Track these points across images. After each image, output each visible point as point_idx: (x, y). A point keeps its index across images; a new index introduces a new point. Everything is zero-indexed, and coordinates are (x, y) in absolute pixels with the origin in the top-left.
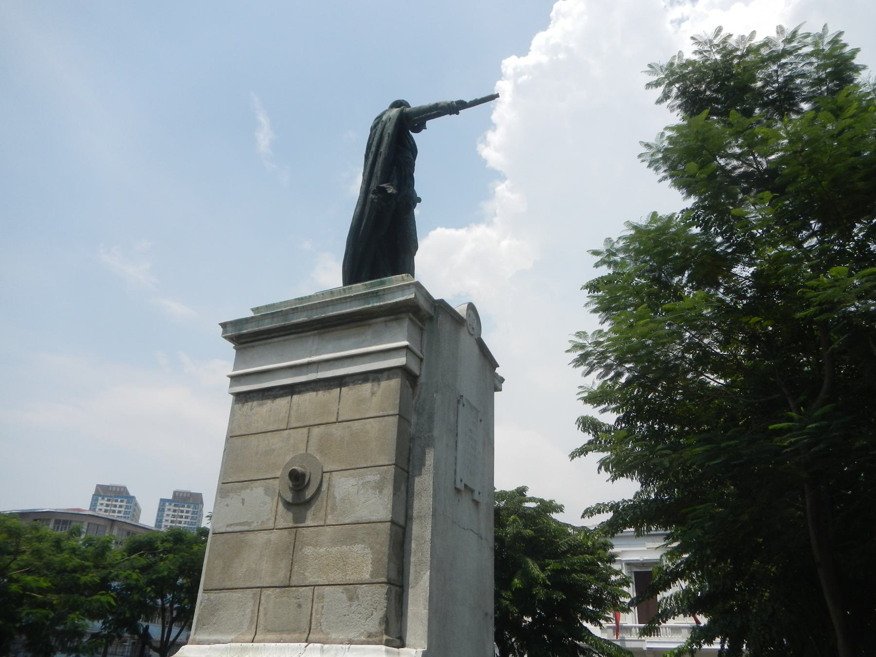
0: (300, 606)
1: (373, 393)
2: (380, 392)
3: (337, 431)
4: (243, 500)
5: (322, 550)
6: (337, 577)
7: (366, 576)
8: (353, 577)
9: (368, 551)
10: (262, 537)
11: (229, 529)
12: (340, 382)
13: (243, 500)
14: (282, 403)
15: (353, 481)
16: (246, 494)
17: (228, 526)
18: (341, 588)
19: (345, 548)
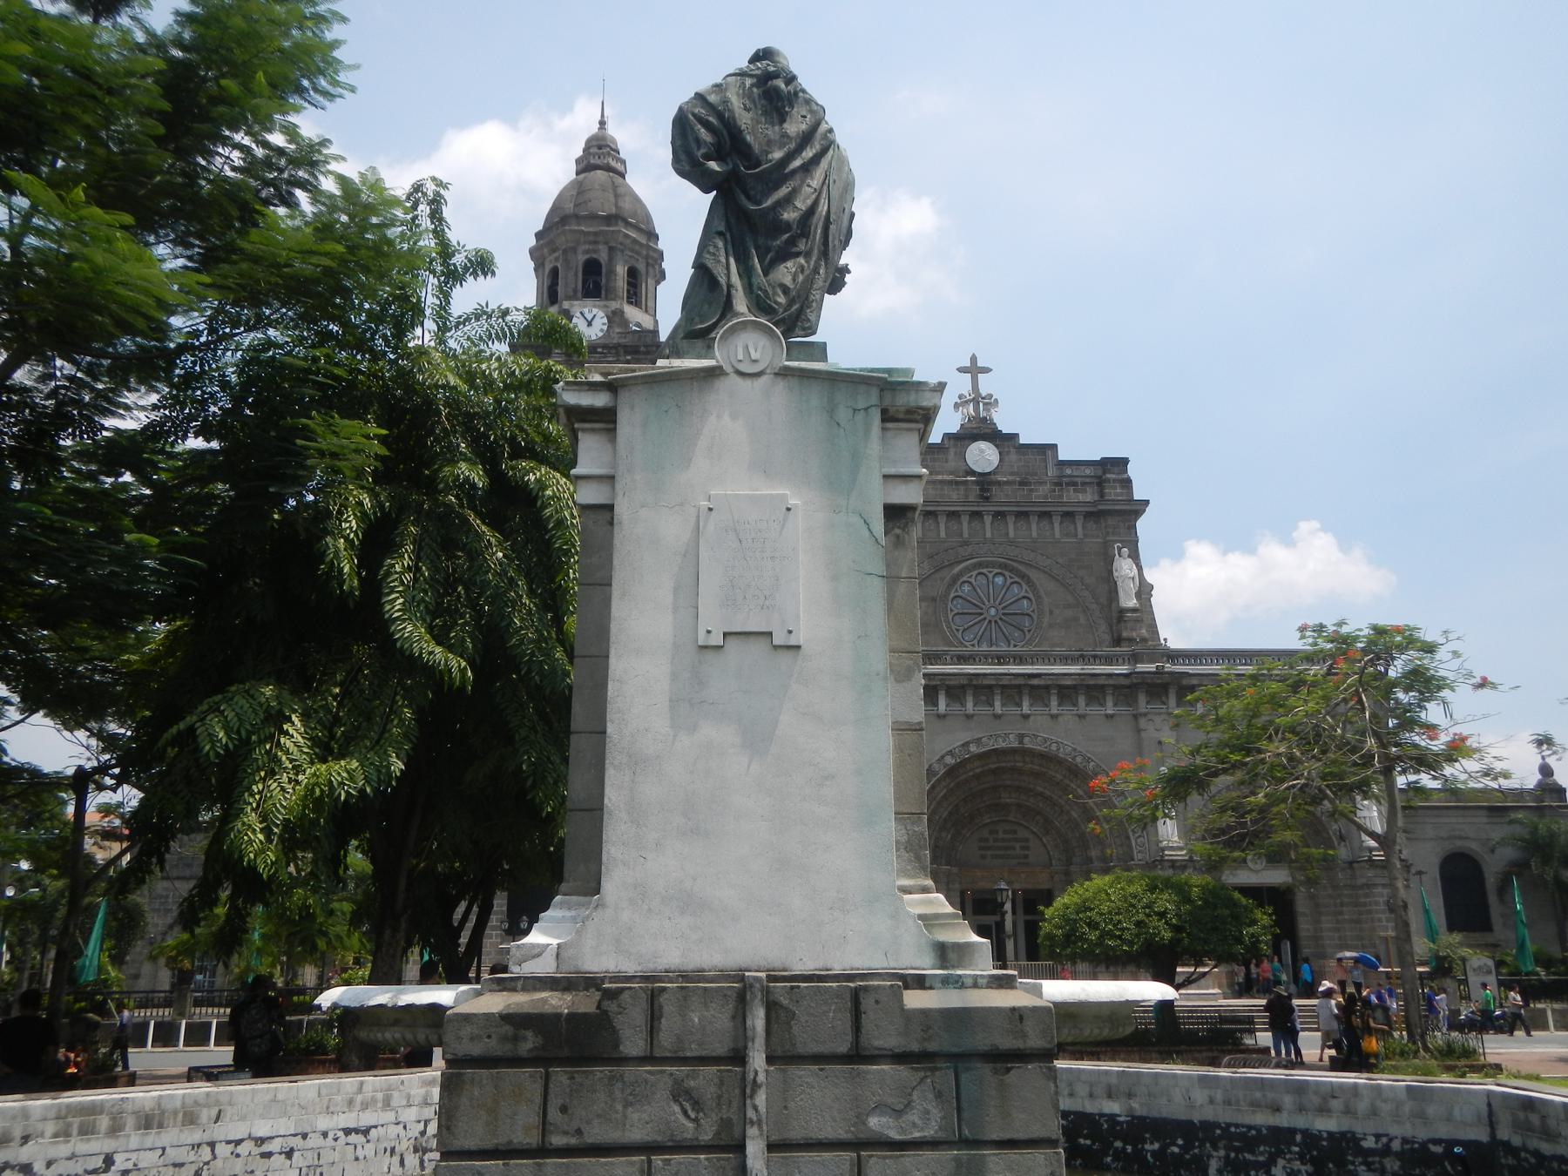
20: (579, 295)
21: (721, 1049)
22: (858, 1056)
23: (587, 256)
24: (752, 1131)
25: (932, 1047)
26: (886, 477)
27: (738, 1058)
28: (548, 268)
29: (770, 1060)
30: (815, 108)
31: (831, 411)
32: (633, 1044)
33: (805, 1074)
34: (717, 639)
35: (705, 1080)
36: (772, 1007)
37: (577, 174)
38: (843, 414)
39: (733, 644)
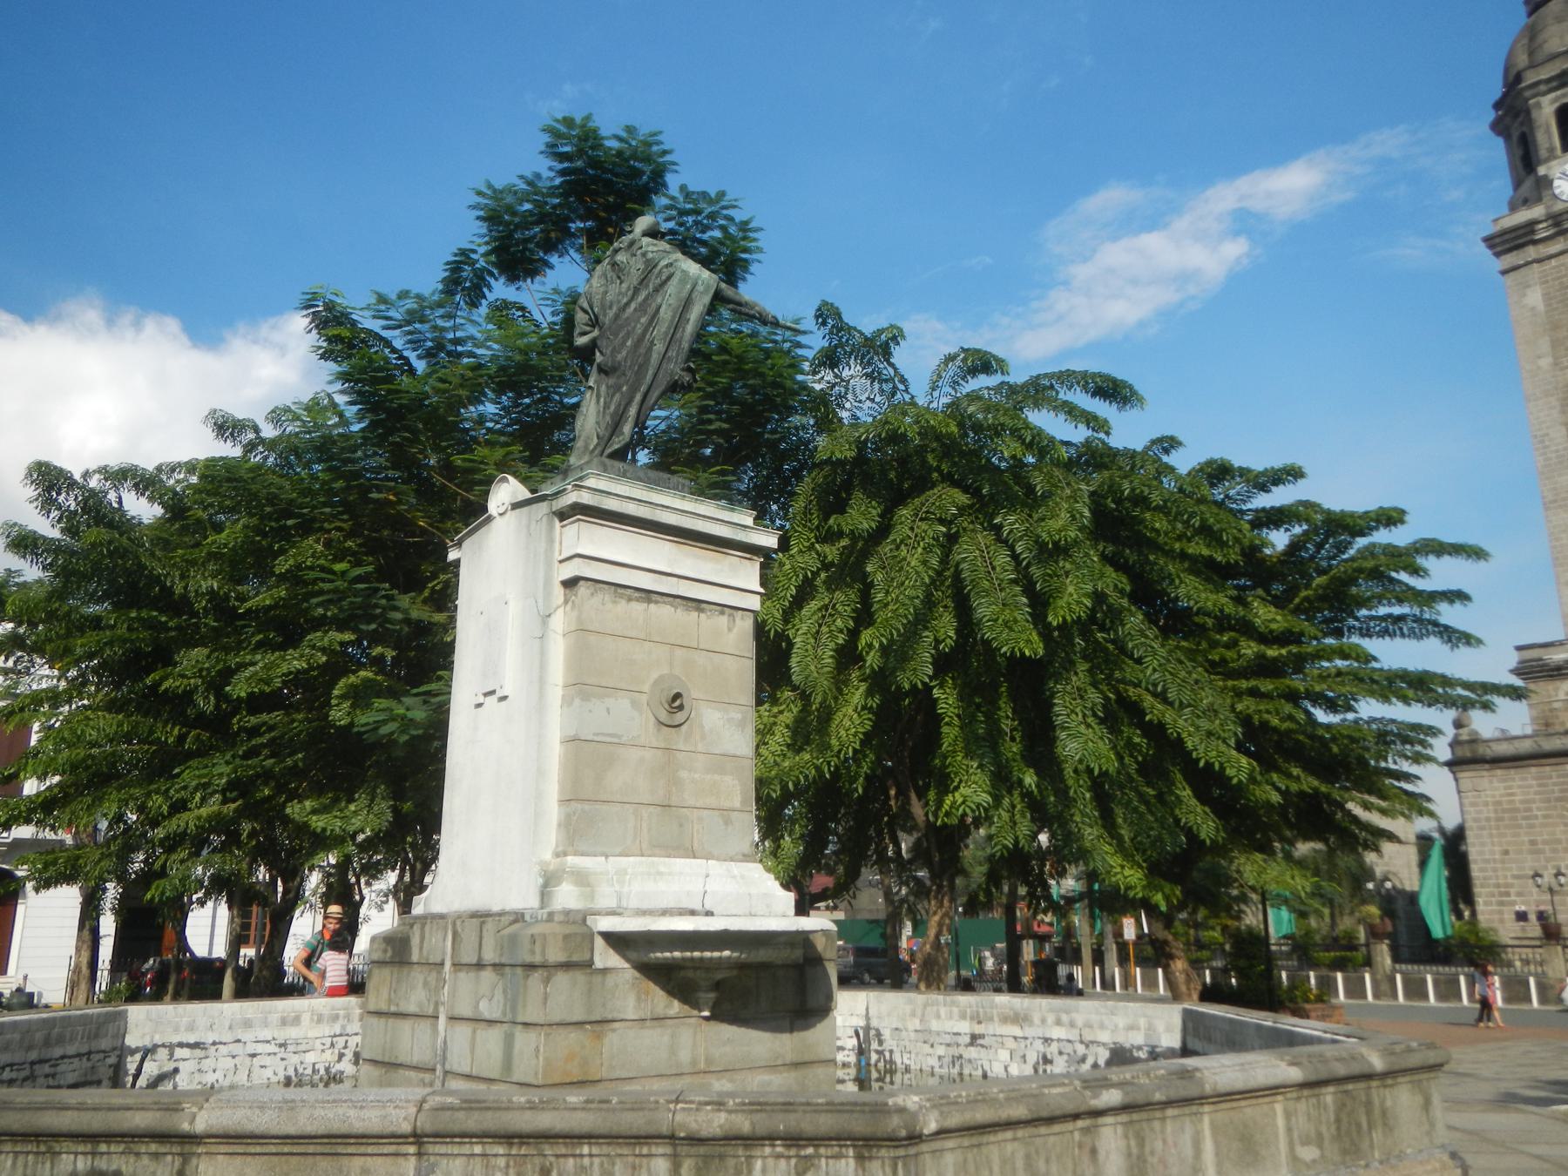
0: (681, 825)
1: (730, 630)
2: (735, 630)
3: (701, 659)
4: (608, 710)
5: (697, 776)
6: (711, 801)
7: (737, 804)
8: (727, 804)
9: (736, 782)
10: (635, 754)
11: (596, 738)
12: (697, 604)
13: (608, 710)
14: (638, 607)
15: (717, 715)
16: (610, 702)
17: (598, 734)
18: (716, 813)
19: (717, 777)
20: (1559, 151)
21: (438, 960)
22: (479, 966)
23: (1557, 105)
24: (441, 1009)
25: (503, 961)
26: (561, 562)
27: (442, 964)
28: (1515, 135)
29: (454, 965)
30: (650, 255)
31: (528, 527)
32: (415, 958)
33: (462, 975)
34: (481, 699)
35: (432, 978)
36: (455, 934)
37: (1530, 14)
38: (533, 526)
39: (489, 699)
